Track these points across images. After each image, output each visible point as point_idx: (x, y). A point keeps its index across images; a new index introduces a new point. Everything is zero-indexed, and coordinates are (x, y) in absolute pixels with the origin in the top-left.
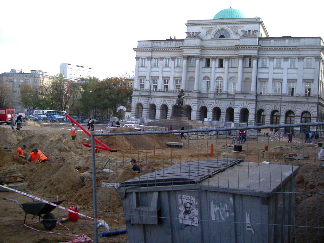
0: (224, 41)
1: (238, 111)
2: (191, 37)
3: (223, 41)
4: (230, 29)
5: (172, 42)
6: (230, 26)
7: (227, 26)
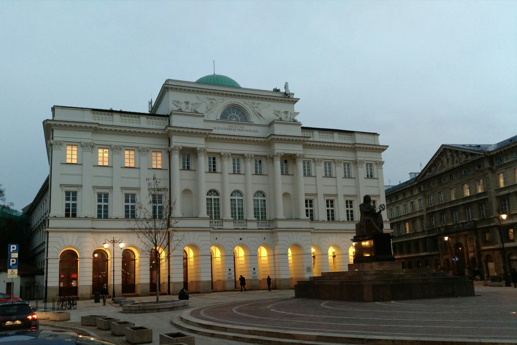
0: (242, 126)
3: (240, 126)
4: (247, 106)
6: (247, 101)
7: (243, 100)
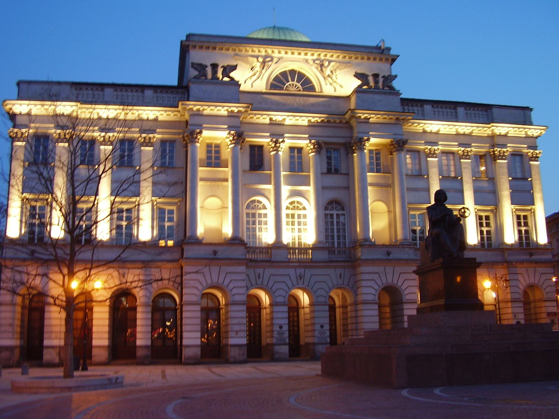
1: (370, 298)
2: (210, 76)
5: (143, 92)
